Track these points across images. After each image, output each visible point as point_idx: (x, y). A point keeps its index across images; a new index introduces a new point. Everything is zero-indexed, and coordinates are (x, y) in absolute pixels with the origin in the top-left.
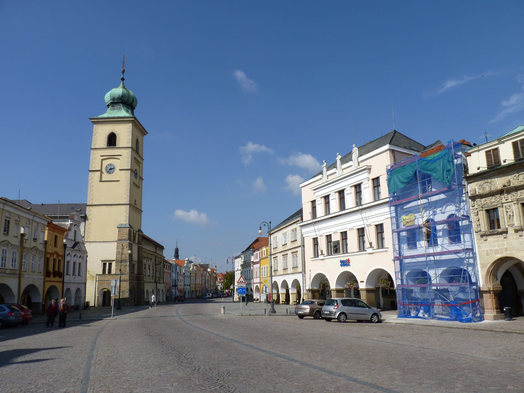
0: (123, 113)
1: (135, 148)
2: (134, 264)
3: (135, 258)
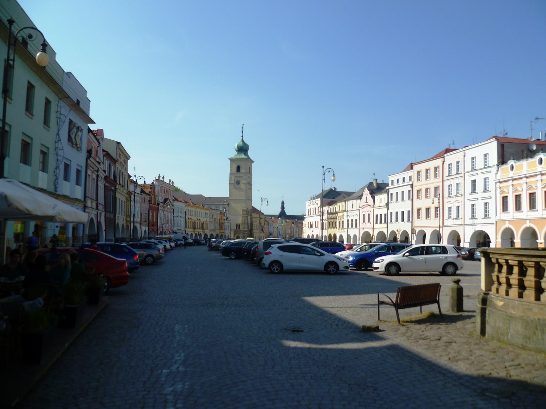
0: (243, 156)
1: (248, 172)
2: (249, 225)
3: (249, 222)
